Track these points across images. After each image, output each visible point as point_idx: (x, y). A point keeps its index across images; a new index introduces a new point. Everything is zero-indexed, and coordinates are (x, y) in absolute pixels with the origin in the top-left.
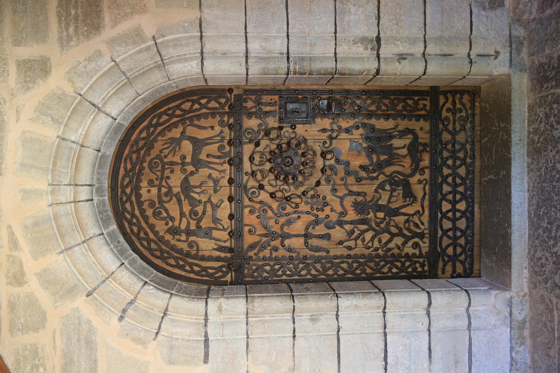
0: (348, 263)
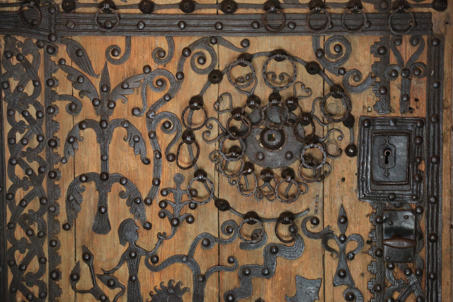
0: (41, 272)
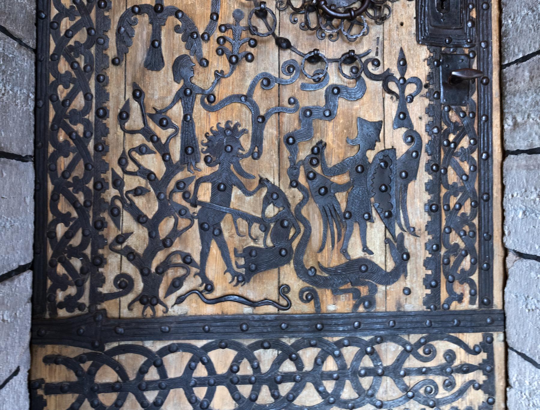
0: (87, 109)
